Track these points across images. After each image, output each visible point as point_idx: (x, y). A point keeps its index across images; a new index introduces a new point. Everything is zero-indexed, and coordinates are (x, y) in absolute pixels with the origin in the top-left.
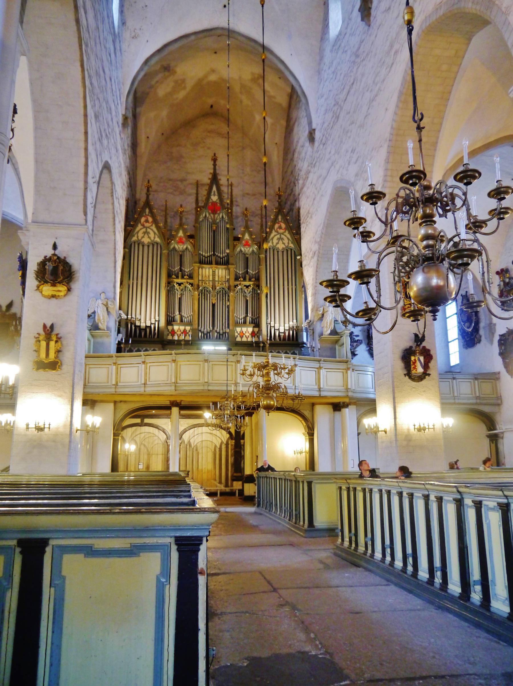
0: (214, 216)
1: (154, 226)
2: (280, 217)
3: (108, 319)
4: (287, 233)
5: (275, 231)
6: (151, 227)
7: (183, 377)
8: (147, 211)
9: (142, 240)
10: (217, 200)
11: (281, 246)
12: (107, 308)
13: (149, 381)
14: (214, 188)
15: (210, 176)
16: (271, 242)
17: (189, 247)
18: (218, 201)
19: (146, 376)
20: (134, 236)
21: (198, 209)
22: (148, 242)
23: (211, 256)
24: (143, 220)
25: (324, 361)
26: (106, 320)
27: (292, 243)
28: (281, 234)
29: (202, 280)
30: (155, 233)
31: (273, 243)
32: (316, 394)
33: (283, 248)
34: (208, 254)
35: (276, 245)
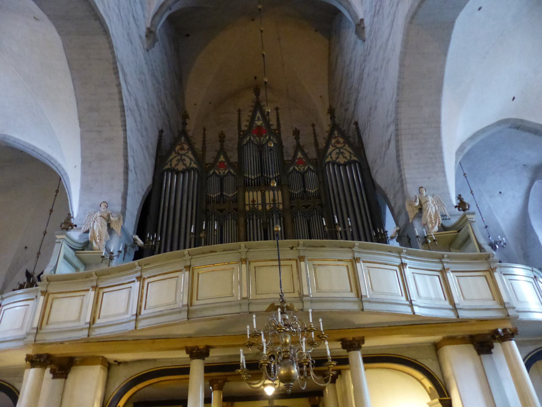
0: (260, 140)
1: (190, 152)
2: (336, 133)
3: (108, 237)
4: (347, 147)
5: (333, 147)
6: (187, 154)
7: (201, 294)
8: (183, 139)
9: (176, 168)
10: (262, 124)
11: (341, 160)
12: (109, 225)
13: (145, 309)
14: (258, 114)
15: (253, 104)
16: (329, 157)
17: (232, 171)
18: (263, 125)
19: (141, 301)
20: (167, 164)
21: (242, 135)
22: (183, 169)
23: (259, 177)
24: (178, 148)
25: (448, 257)
26: (103, 238)
27: (354, 156)
28: (339, 148)
29: (249, 204)
30: (191, 160)
31: (331, 158)
32: (450, 315)
33: (344, 161)
34: (256, 176)
35: (336, 160)
